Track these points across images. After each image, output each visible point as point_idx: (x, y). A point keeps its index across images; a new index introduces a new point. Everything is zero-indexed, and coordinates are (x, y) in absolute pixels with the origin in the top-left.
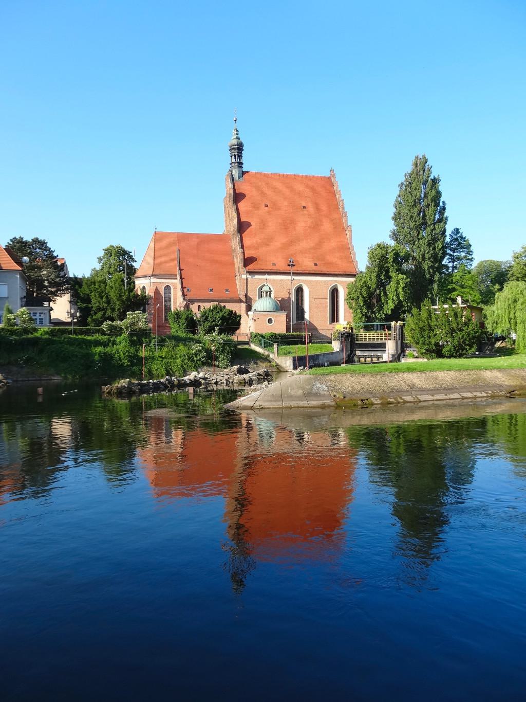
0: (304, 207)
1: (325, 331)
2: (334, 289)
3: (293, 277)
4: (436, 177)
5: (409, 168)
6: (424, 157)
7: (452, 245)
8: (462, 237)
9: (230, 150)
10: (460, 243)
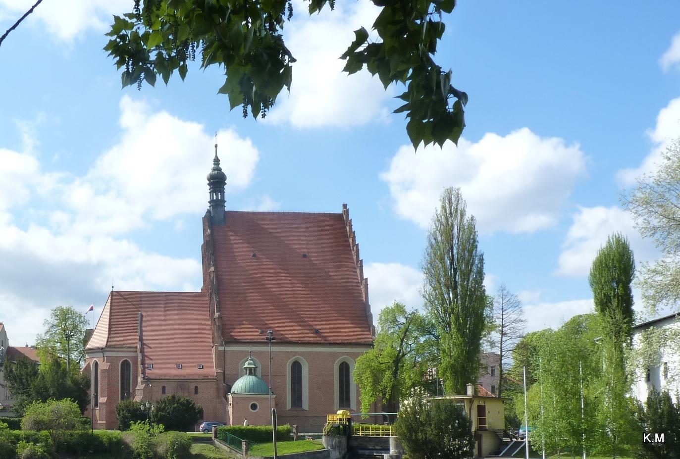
9: (208, 184)
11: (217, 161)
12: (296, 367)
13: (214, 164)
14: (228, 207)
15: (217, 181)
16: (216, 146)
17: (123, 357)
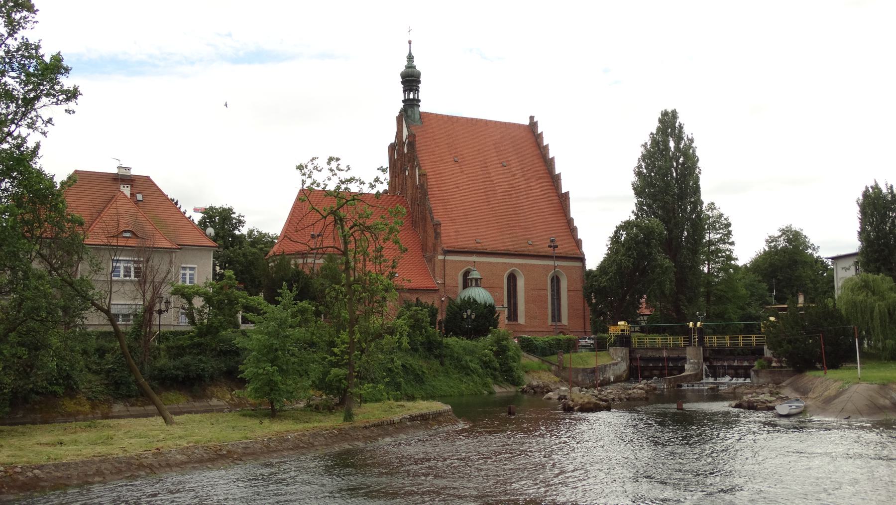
3: (558, 263)
8: (721, 215)
9: (402, 83)
11: (410, 58)
12: (512, 279)
13: (409, 61)
14: (424, 107)
15: (411, 80)
16: (410, 43)
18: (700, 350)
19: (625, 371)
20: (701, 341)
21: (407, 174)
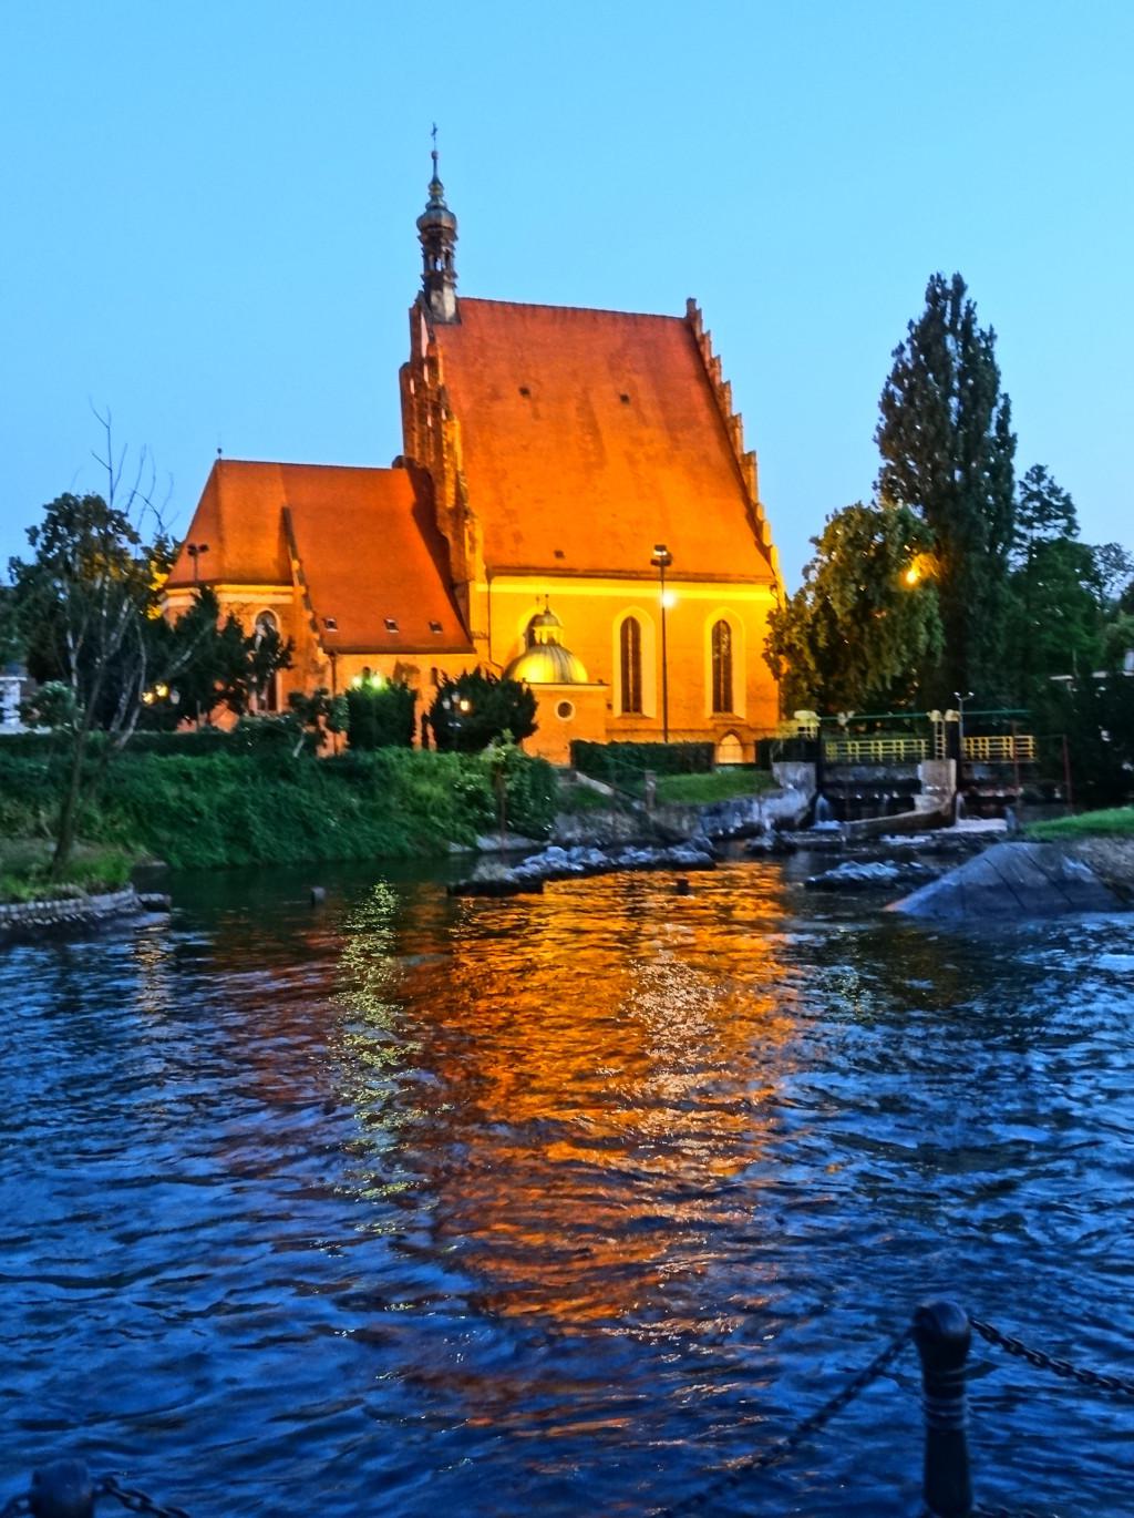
0: (624, 399)
1: (697, 735)
2: (719, 623)
4: (986, 330)
5: (919, 309)
6: (958, 281)
7: (1025, 508)
8: (1054, 491)
10: (1046, 504)
11: (435, 185)
12: (631, 629)
15: (436, 234)
16: (434, 156)
17: (260, 605)
18: (948, 767)
19: (803, 809)
20: (954, 751)
21: (430, 423)
